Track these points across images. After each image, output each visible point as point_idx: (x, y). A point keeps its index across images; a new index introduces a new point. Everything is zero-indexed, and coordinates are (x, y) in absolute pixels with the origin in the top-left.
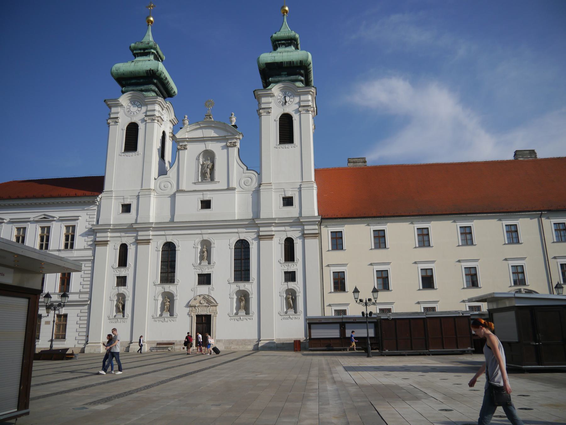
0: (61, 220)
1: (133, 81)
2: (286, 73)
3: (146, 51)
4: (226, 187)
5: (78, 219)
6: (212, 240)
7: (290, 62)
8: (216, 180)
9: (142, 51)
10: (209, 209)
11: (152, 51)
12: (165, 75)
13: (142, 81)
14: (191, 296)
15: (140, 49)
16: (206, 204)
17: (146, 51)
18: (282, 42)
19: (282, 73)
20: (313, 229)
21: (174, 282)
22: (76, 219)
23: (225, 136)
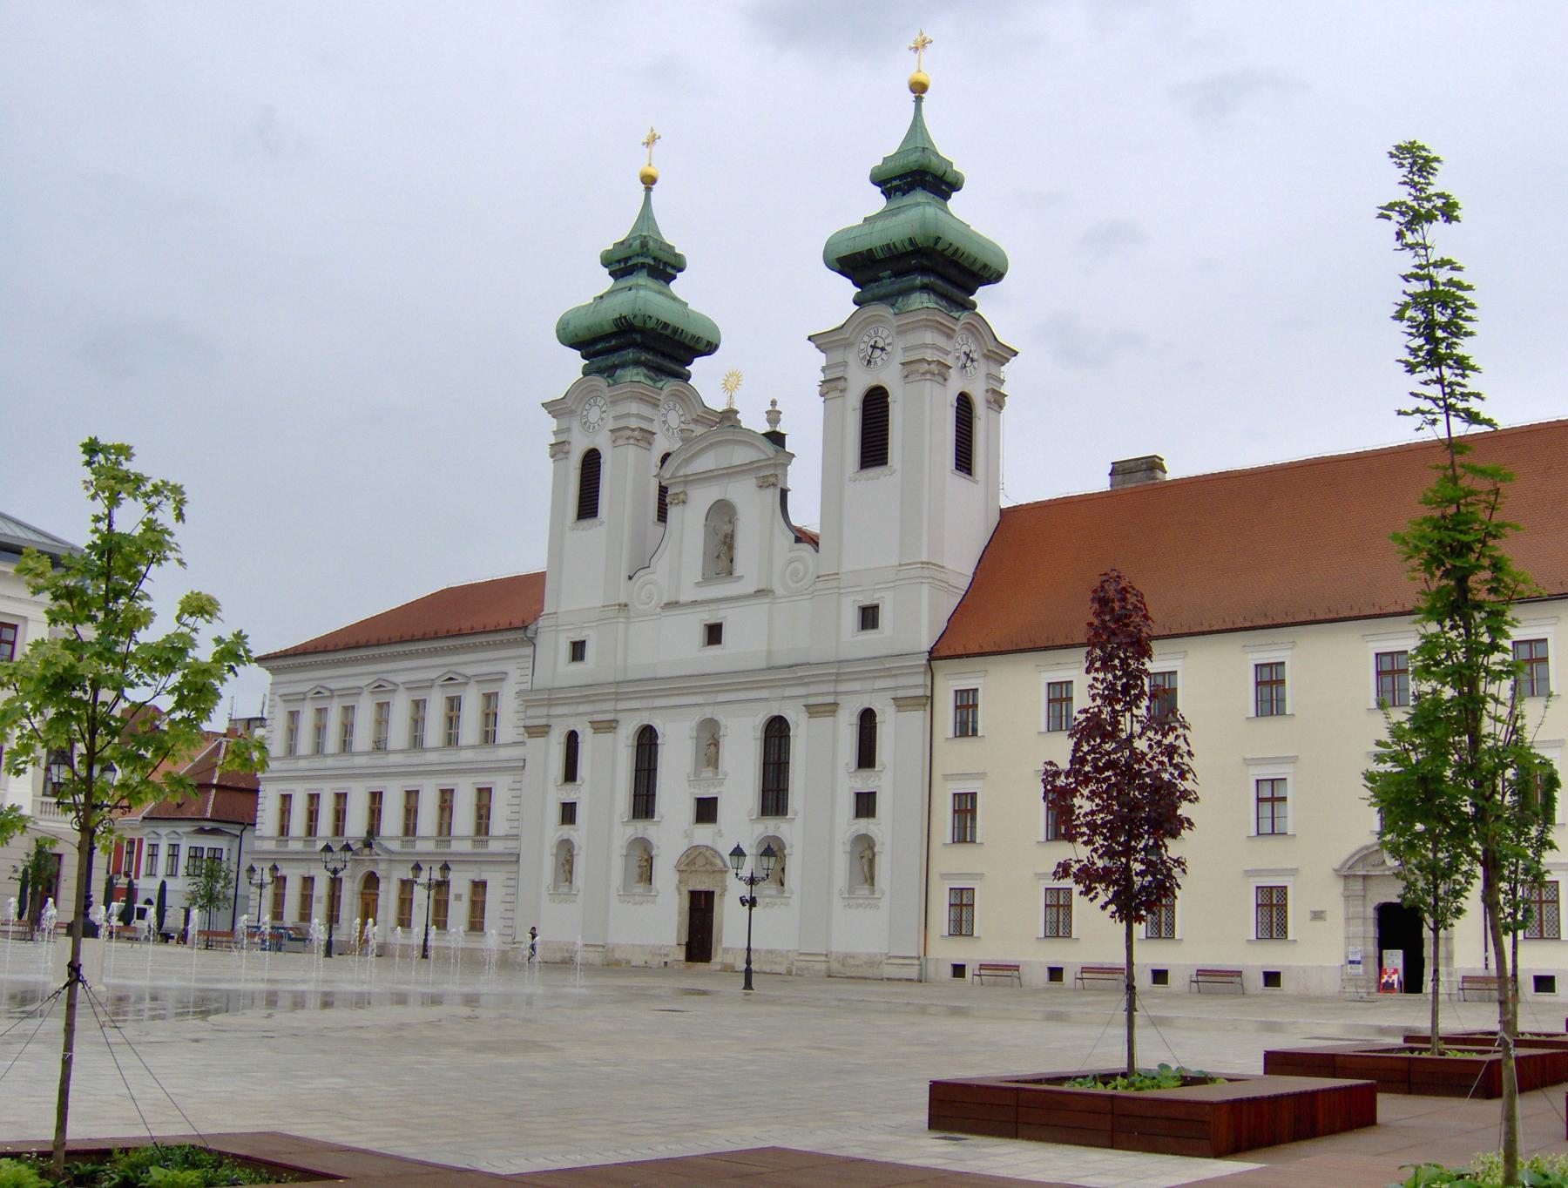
0: (482, 680)
1: (599, 346)
2: (889, 272)
3: (630, 263)
4: (751, 590)
5: (502, 680)
6: (721, 719)
7: (888, 245)
8: (737, 573)
9: (622, 265)
10: (717, 646)
11: (641, 260)
12: (658, 320)
13: (613, 342)
14: (683, 846)
15: (619, 261)
16: (714, 634)
17: (630, 263)
18: (894, 183)
19: (880, 275)
20: (915, 684)
21: (653, 817)
22: (501, 677)
23: (752, 463)
